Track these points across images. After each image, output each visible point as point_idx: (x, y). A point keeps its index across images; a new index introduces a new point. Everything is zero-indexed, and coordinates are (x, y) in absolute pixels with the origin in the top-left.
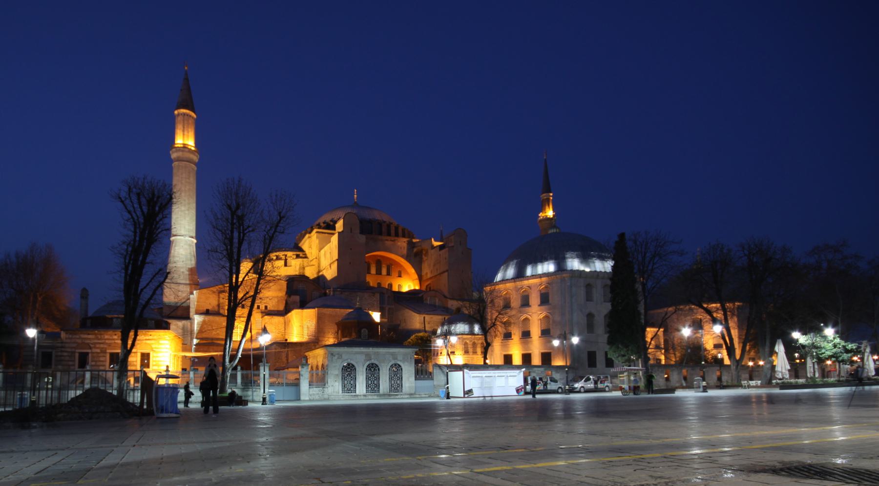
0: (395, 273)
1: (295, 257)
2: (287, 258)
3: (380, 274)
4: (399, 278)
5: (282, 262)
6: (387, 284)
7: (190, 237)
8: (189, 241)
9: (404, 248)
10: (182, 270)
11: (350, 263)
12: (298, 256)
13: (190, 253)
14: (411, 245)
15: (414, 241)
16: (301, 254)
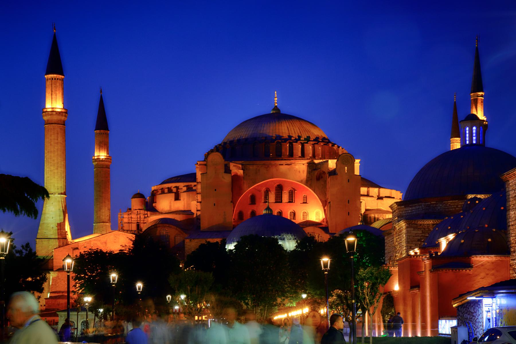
0: (299, 199)
1: (185, 189)
2: (179, 190)
3: (281, 202)
4: (304, 204)
5: (172, 195)
6: (289, 213)
7: (59, 194)
8: (58, 197)
9: (303, 171)
10: (52, 226)
11: (215, 205)
12: (189, 189)
13: (59, 209)
14: (312, 167)
15: (316, 161)
16: (193, 184)
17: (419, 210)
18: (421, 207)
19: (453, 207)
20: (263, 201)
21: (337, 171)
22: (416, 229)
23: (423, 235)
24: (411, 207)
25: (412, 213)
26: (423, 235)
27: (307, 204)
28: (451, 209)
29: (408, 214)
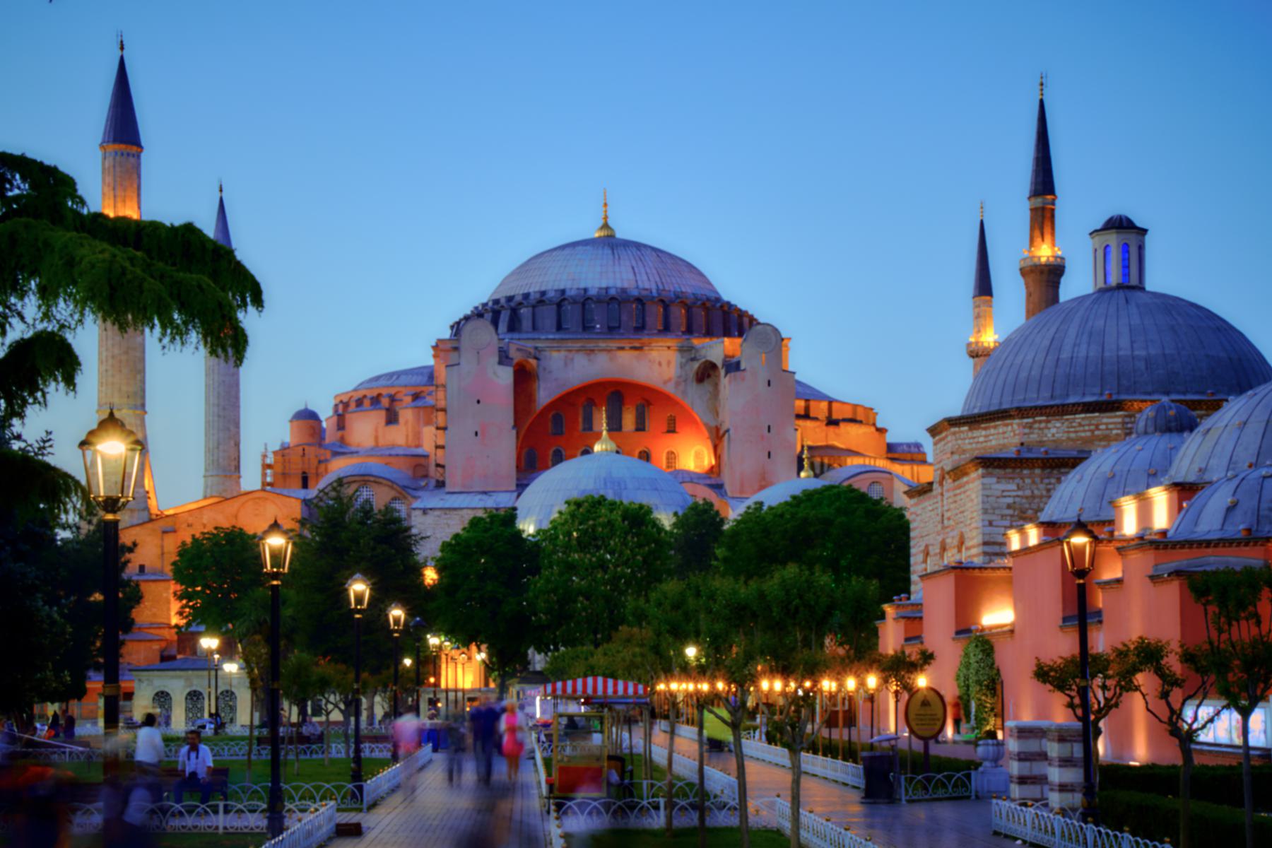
0: (656, 420)
9: (669, 363)
17: (1006, 435)
18: (1010, 428)
19: (1087, 428)
20: (581, 427)
21: (743, 366)
22: (1003, 481)
23: (1020, 493)
24: (985, 429)
25: (989, 444)
26: (1020, 493)
27: (675, 436)
28: (1083, 434)
29: (979, 446)
